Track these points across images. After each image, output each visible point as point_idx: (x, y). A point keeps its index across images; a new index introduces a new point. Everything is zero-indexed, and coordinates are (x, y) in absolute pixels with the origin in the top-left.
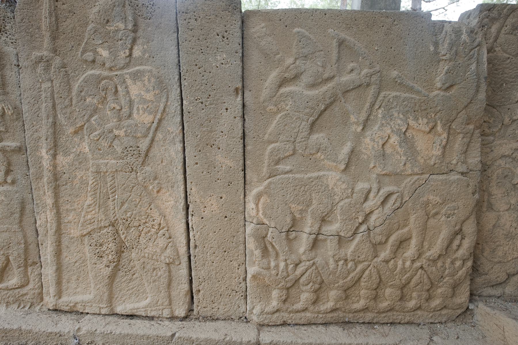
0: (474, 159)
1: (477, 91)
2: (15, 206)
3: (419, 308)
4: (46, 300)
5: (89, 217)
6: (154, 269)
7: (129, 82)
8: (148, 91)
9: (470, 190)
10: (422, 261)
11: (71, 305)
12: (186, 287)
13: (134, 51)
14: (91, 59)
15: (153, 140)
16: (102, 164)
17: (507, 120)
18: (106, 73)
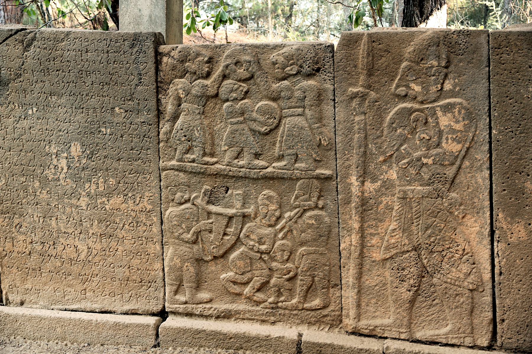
2: (324, 229)
4: (346, 323)
5: (393, 241)
6: (457, 295)
7: (439, 113)
8: (457, 122)
11: (371, 328)
12: (490, 315)
13: (445, 85)
14: (403, 93)
15: (460, 168)
16: (409, 190)
18: (417, 106)
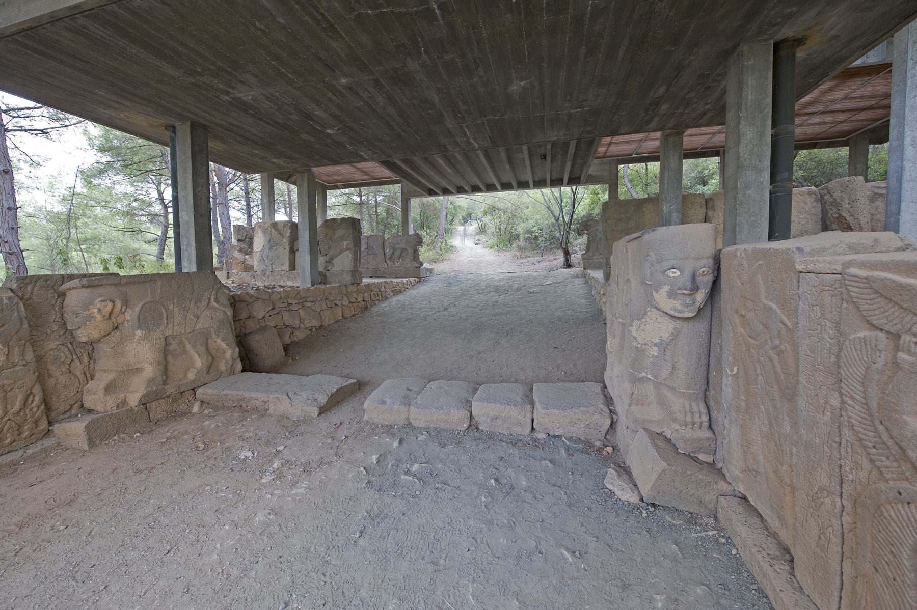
0: (30, 356)
1: (22, 324)
3: (15, 441)
9: (31, 372)
10: (9, 416)
17: (49, 332)
